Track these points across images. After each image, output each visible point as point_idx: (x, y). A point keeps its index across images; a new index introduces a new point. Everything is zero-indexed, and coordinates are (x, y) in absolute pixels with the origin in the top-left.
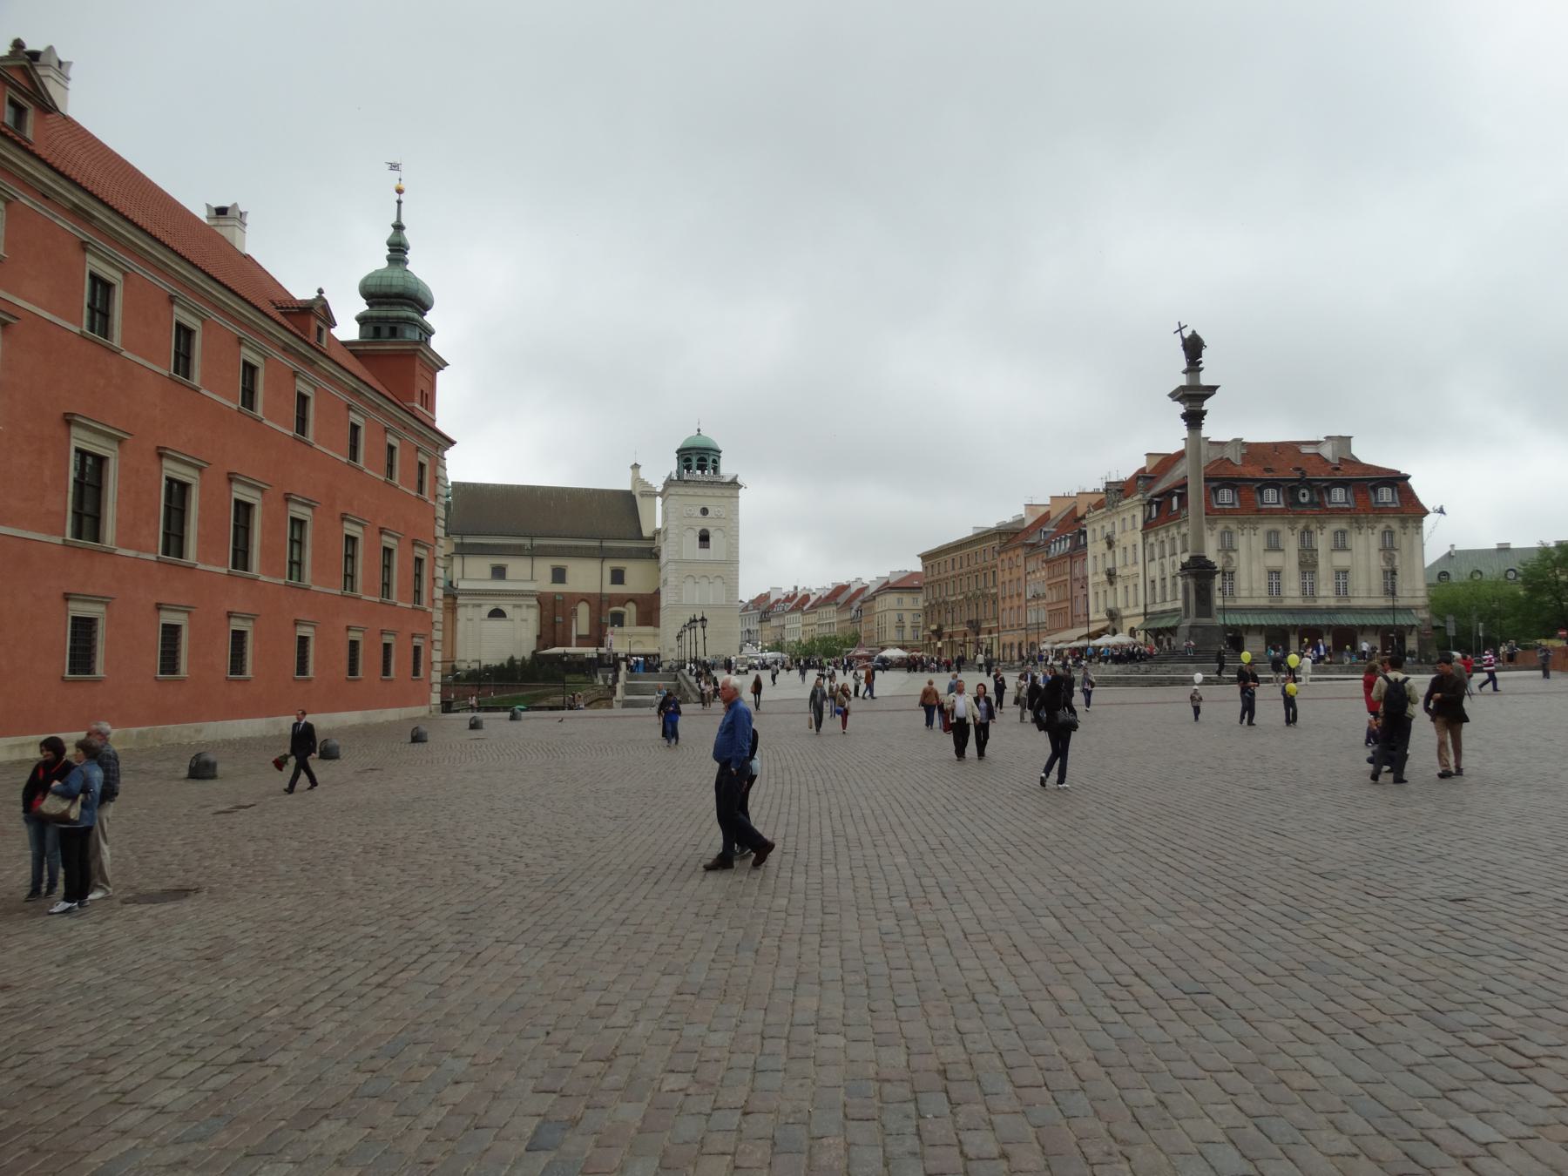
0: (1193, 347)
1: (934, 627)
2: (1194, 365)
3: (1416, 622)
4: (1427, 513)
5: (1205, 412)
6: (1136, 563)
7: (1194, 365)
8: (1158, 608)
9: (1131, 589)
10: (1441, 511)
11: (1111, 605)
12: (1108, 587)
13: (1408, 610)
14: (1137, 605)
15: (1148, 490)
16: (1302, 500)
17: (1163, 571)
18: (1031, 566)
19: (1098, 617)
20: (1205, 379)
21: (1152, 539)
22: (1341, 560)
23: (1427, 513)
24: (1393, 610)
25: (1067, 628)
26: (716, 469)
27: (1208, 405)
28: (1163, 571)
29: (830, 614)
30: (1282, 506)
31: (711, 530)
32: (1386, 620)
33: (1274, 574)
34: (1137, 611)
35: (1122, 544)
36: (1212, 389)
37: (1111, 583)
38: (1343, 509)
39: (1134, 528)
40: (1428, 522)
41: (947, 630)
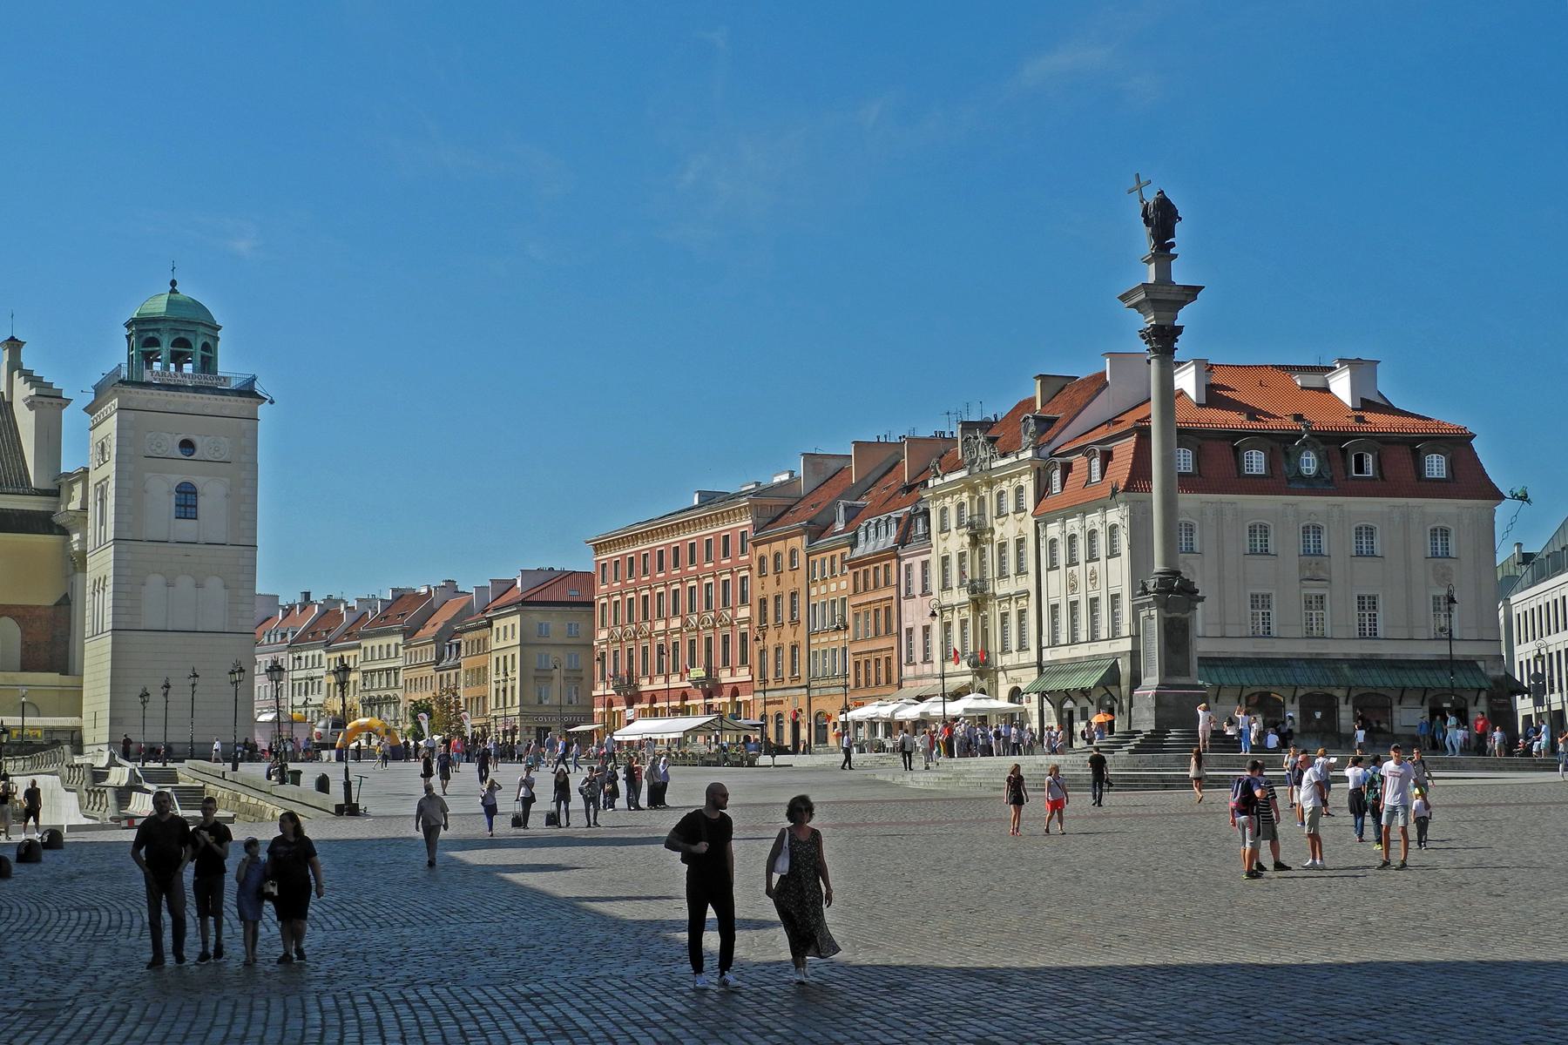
0: (1162, 219)
2: (1163, 250)
3: (1484, 684)
4: (1504, 498)
5: (1179, 330)
6: (1021, 571)
7: (1163, 250)
8: (1063, 653)
10: (1524, 498)
12: (967, 613)
13: (1469, 664)
14: (1022, 647)
20: (1180, 275)
21: (1053, 530)
23: (1504, 498)
24: (1451, 664)
26: (208, 364)
27: (1183, 317)
28: (1073, 587)
29: (385, 650)
31: (197, 481)
32: (1442, 680)
33: (1260, 601)
35: (996, 537)
36: (1192, 292)
39: (1019, 509)
40: (1503, 511)
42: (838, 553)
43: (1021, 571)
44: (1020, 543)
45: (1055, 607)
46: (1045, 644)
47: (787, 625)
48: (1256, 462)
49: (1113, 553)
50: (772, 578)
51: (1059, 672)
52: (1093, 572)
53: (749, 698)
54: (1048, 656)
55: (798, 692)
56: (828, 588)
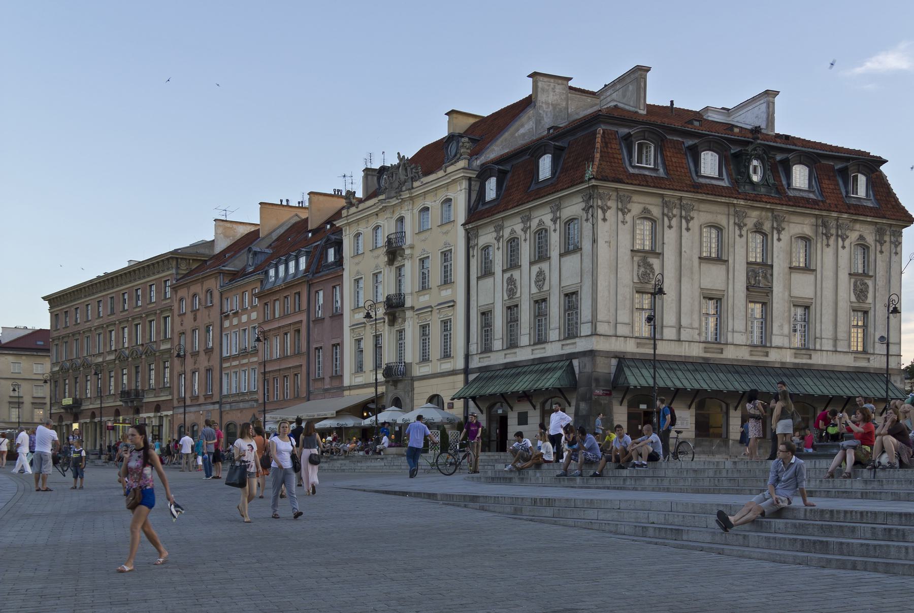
1: (68, 401)
6: (447, 281)
8: (497, 359)
9: (435, 332)
11: (389, 357)
15: (475, 154)
16: (755, 178)
17: (511, 292)
18: (233, 303)
19: (359, 380)
21: (487, 237)
22: (803, 286)
25: (297, 398)
28: (511, 292)
30: (725, 183)
34: (447, 366)
37: (392, 321)
38: (807, 200)
39: (447, 222)
41: (87, 406)
42: (249, 288)
43: (447, 281)
44: (446, 255)
45: (486, 315)
46: (473, 349)
47: (202, 353)
48: (709, 163)
49: (570, 248)
50: (190, 316)
51: (492, 378)
52: (540, 273)
53: (170, 413)
54: (475, 363)
55: (211, 407)
56: (240, 320)
